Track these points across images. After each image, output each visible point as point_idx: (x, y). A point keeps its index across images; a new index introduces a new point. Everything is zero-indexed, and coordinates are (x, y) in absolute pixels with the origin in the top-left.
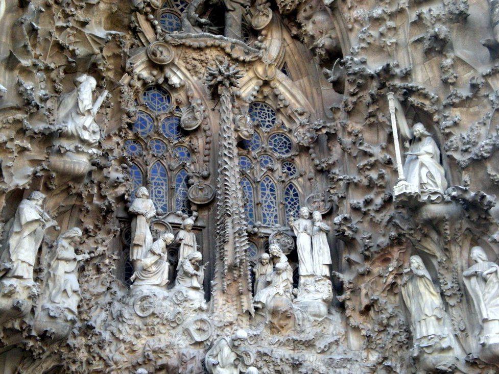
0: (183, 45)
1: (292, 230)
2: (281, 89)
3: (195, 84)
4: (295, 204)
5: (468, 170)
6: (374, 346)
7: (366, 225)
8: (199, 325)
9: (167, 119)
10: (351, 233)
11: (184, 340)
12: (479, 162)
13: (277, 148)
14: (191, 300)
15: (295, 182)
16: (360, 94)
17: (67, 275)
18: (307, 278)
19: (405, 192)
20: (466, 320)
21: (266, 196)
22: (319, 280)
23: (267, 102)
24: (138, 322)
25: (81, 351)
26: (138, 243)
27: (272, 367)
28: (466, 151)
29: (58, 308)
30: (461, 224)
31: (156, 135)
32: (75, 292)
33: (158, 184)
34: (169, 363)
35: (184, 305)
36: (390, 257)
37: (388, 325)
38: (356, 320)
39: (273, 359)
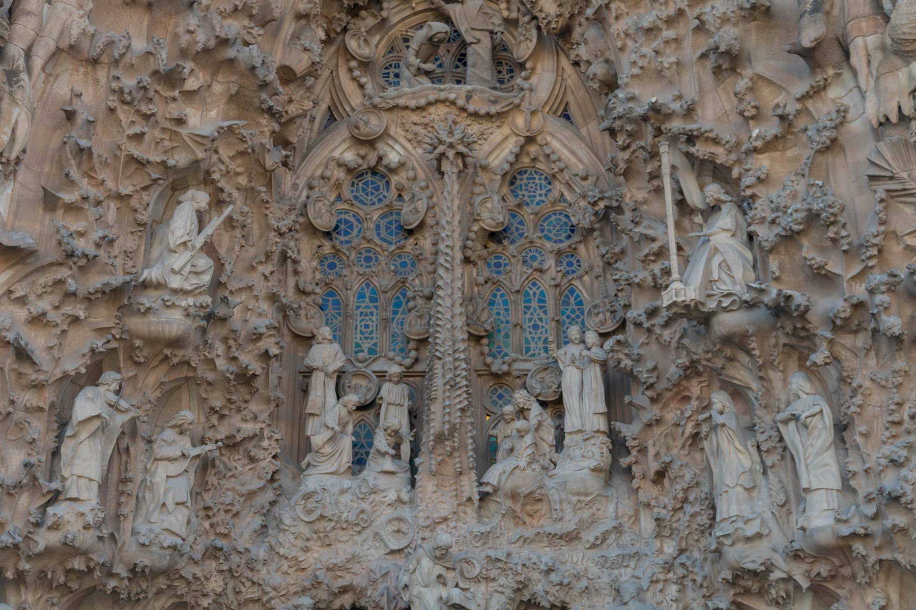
0: (396, 107)
1: (556, 362)
2: (555, 144)
3: (420, 160)
4: (578, 317)
5: (778, 253)
6: (666, 532)
7: (654, 347)
8: (395, 526)
9: (383, 217)
10: (630, 363)
11: (377, 548)
12: (790, 238)
13: (551, 235)
14: (383, 491)
15: (577, 283)
16: (634, 147)
17: (171, 480)
18: (574, 436)
19: (675, 302)
20: (790, 489)
21: (532, 310)
22: (587, 439)
23: (539, 165)
24: (304, 530)
25: (212, 580)
26: (312, 412)
27: (511, 576)
28: (773, 222)
29: (151, 531)
30: (775, 337)
31: (364, 242)
32: (177, 504)
33: (366, 315)
34: (355, 583)
35: (371, 500)
36: (689, 394)
37: (685, 500)
38: (648, 492)
39: (511, 566)
